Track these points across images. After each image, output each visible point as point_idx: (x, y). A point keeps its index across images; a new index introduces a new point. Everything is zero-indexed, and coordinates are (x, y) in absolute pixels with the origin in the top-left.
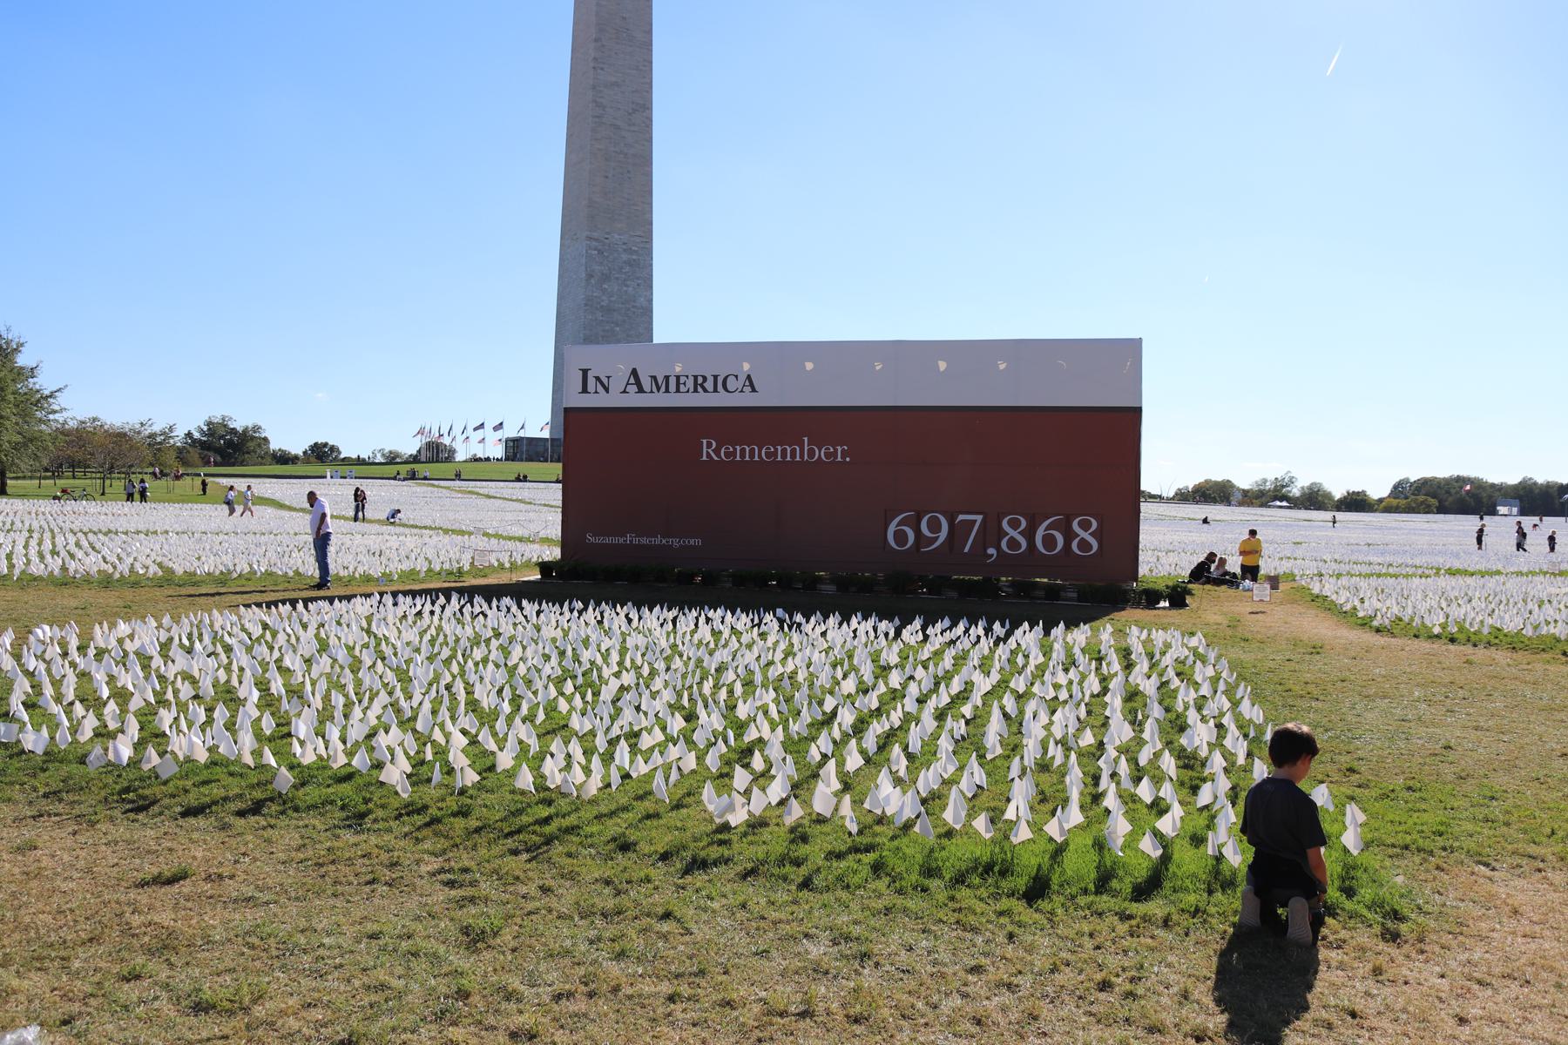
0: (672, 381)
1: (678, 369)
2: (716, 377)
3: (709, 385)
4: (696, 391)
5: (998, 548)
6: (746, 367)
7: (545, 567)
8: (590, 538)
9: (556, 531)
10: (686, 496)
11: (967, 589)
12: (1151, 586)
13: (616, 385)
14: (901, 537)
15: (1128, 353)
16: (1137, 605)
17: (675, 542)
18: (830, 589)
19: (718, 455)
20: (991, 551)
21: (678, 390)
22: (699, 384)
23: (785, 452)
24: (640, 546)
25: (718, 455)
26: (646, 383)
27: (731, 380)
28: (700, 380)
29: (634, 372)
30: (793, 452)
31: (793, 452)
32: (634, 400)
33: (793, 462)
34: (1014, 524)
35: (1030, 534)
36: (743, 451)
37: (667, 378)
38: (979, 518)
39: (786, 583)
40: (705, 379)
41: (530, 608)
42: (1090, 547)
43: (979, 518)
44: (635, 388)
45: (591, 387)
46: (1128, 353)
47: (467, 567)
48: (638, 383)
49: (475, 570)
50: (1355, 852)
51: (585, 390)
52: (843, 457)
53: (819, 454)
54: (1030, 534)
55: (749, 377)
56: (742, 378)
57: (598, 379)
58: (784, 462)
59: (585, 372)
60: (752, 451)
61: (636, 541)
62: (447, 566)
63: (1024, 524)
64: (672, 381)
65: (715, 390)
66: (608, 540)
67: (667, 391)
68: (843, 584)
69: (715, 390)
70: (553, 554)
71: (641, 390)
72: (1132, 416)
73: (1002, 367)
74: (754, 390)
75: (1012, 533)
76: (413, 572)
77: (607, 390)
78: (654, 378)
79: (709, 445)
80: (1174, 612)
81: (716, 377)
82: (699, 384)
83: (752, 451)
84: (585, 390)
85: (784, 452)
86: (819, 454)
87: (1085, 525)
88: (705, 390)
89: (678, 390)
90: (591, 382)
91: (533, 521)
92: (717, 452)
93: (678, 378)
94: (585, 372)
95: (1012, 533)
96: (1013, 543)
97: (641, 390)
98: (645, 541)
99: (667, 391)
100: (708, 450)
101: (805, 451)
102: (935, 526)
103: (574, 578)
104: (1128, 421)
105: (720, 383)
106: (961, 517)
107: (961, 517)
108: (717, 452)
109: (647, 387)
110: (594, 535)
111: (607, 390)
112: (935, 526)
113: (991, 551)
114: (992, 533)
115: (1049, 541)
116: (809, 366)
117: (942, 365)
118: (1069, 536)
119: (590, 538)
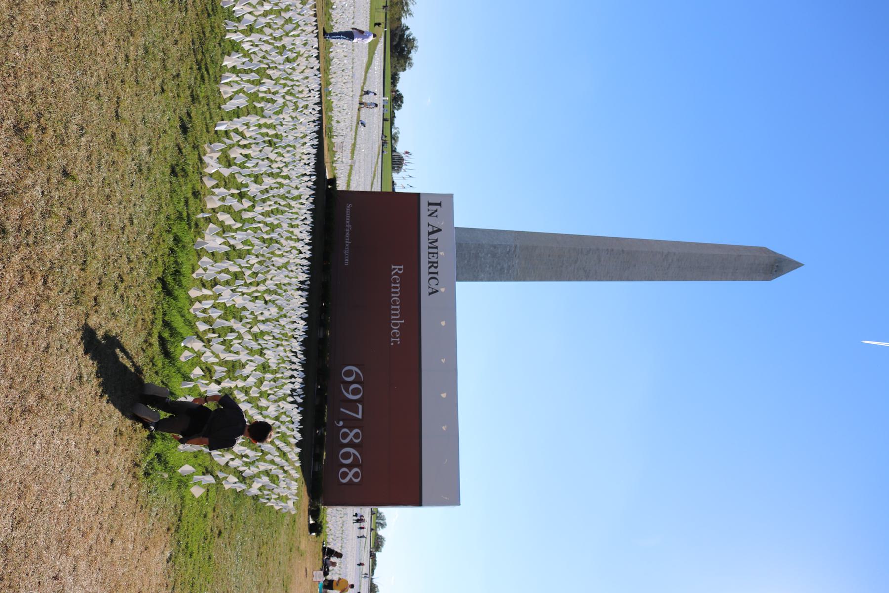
0: (434, 250)
1: (441, 253)
2: (437, 273)
3: (432, 270)
4: (429, 263)
5: (343, 427)
6: (443, 290)
7: (333, 181)
8: (349, 206)
10: (371, 263)
11: (320, 411)
12: (321, 514)
13: (432, 220)
15: (452, 498)
16: (311, 504)
17: (346, 251)
18: (321, 334)
19: (395, 274)
20: (341, 423)
21: (430, 253)
23: (396, 310)
24: (345, 233)
25: (395, 274)
26: (433, 236)
27: (435, 281)
28: (435, 265)
29: (439, 230)
30: (396, 315)
31: (396, 315)
32: (424, 230)
33: (390, 315)
34: (356, 436)
35: (351, 444)
36: (396, 288)
37: (436, 247)
38: (360, 416)
39: (324, 311)
40: (436, 267)
41: (309, 170)
42: (344, 478)
43: (360, 416)
44: (431, 230)
45: (431, 207)
46: (452, 498)
47: (334, 140)
48: (433, 232)
49: (332, 145)
50: (179, 471)
51: (430, 204)
52: (394, 342)
53: (395, 329)
54: (351, 444)
55: (437, 291)
56: (436, 288)
57: (436, 211)
59: (439, 204)
60: (396, 292)
61: (347, 230)
62: (334, 128)
63: (357, 441)
64: (434, 250)
65: (430, 273)
66: (348, 215)
67: (429, 247)
68: (323, 341)
69: (430, 273)
70: (341, 186)
71: (430, 233)
72: (419, 503)
73: (444, 428)
74: (430, 294)
75: (351, 435)
76: (331, 110)
77: (430, 215)
78: (436, 241)
79: (400, 270)
80: (307, 528)
81: (437, 273)
82: (433, 264)
83: (396, 292)
84: (430, 204)
85: (396, 310)
86: (395, 329)
87: (356, 475)
88: (430, 268)
89: (430, 253)
90: (434, 207)
91: (357, 174)
92: (396, 274)
93: (436, 253)
94: (439, 204)
95: (351, 435)
96: (345, 435)
97: (430, 233)
98: (347, 235)
99: (429, 247)
100: (397, 269)
101: (396, 321)
102: (355, 392)
103: (328, 199)
105: (433, 276)
106: (360, 407)
107: (360, 407)
108: (396, 274)
109: (432, 236)
110: (351, 208)
111: (430, 215)
112: (355, 392)
113: (341, 423)
114: (351, 423)
115: (347, 455)
116: (443, 323)
117: (444, 395)
118: (350, 467)
119: (349, 206)
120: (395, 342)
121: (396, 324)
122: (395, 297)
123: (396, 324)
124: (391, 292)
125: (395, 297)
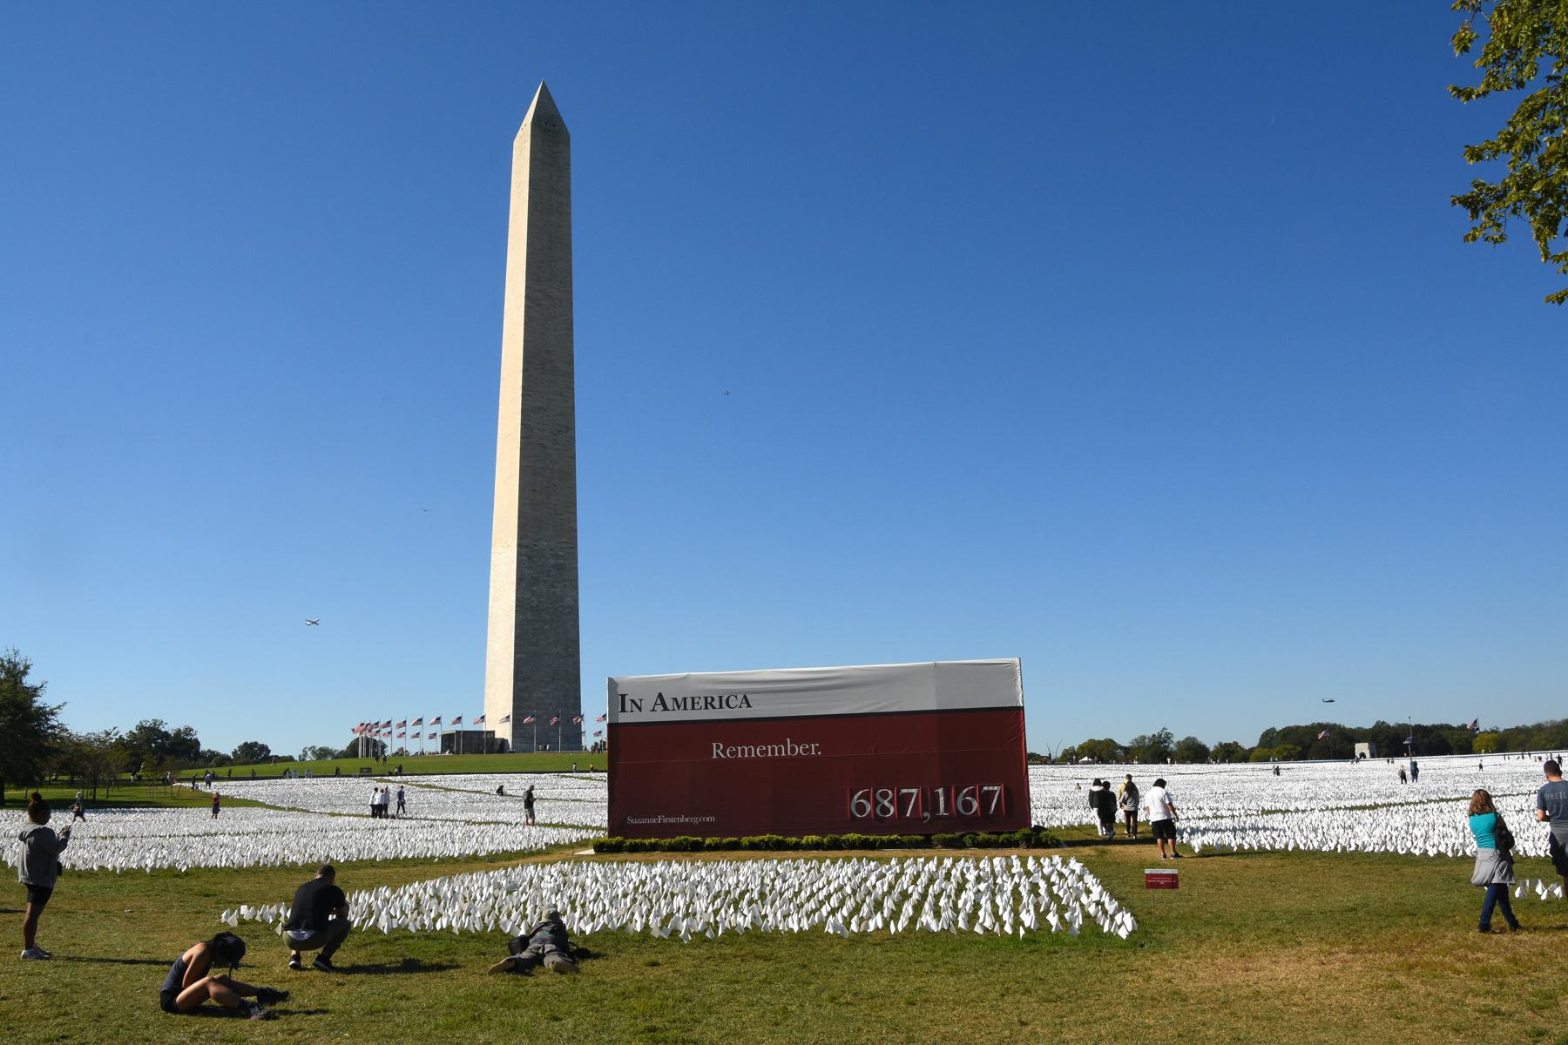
0: (689, 702)
9: (601, 817)
13: (647, 706)
14: (861, 808)
22: (709, 703)
23: (774, 751)
26: (669, 703)
29: (660, 696)
32: (661, 716)
45: (628, 707)
53: (799, 750)
56: (740, 697)
58: (773, 758)
59: (623, 696)
64: (689, 702)
82: (709, 703)
84: (623, 710)
86: (799, 750)
92: (724, 751)
97: (665, 708)
98: (672, 820)
100: (717, 751)
104: (1013, 716)
108: (724, 751)
120: (817, 749)
121: (793, 750)
122: (756, 752)
123: (793, 750)
124: (750, 760)
125: (756, 752)
